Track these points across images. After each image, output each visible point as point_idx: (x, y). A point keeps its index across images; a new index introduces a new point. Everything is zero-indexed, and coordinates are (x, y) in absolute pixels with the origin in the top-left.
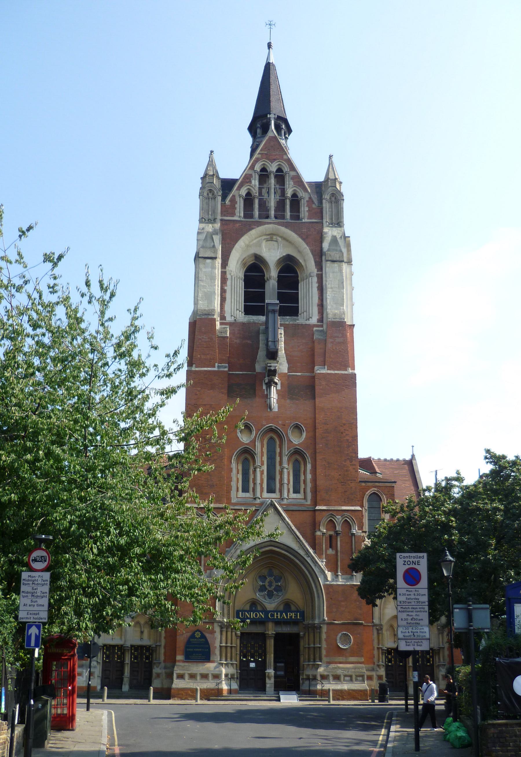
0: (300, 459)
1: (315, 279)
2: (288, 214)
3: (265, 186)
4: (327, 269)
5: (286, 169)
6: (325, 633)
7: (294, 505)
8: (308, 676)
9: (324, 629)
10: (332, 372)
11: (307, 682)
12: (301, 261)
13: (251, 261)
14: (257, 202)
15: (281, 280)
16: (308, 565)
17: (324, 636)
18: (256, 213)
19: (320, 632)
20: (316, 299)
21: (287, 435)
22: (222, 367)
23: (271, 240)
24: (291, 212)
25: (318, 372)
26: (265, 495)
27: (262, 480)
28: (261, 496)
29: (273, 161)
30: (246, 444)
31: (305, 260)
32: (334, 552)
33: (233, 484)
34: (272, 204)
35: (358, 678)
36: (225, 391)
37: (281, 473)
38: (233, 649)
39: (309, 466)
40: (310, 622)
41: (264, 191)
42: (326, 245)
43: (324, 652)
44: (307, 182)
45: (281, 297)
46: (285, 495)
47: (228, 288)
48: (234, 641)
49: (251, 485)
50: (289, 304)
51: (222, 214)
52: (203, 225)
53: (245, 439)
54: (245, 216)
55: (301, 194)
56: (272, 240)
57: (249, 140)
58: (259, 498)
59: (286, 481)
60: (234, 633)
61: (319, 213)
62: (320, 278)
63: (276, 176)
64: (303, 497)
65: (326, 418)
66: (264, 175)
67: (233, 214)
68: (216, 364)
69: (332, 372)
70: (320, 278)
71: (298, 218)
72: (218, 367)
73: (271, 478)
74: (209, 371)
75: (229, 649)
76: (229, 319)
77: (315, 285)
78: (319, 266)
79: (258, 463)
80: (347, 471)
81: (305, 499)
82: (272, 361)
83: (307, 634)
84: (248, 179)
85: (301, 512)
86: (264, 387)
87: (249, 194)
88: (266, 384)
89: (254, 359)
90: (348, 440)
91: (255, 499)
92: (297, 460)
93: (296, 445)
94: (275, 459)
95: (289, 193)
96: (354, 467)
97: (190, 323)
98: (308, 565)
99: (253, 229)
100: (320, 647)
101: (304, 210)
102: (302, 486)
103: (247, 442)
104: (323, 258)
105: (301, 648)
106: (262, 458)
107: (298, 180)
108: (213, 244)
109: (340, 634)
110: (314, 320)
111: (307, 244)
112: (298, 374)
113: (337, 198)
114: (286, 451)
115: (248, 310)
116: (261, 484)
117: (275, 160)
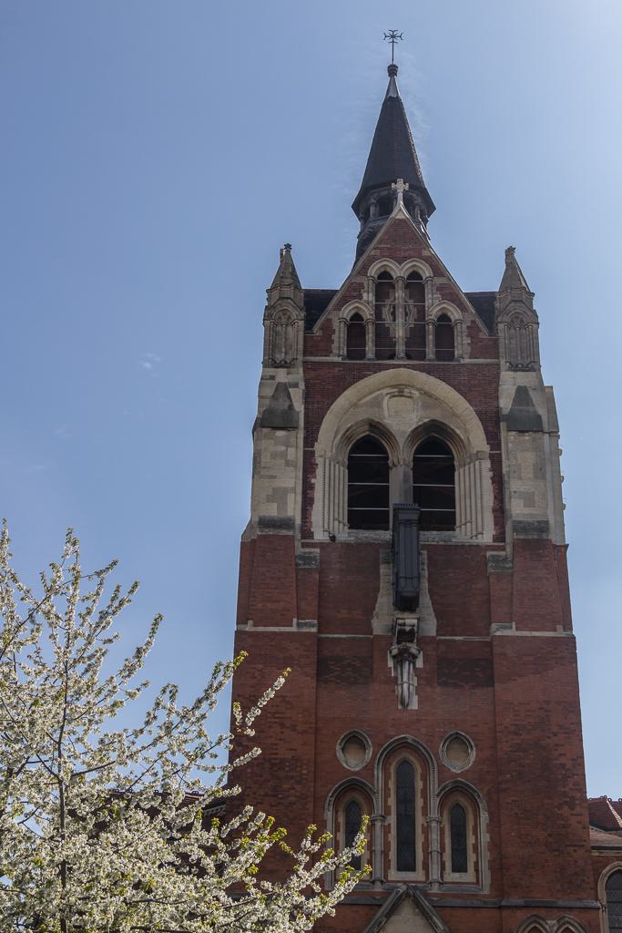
0: (463, 801)
1: (487, 464)
2: (430, 350)
3: (388, 302)
4: (510, 445)
5: (426, 272)
7: (455, 896)
12: (458, 432)
13: (363, 432)
14: (370, 330)
18: (370, 348)
20: (489, 500)
21: (436, 754)
22: (306, 624)
23: (401, 394)
24: (437, 345)
25: (498, 633)
26: (394, 875)
28: (386, 876)
29: (400, 261)
31: (466, 431)
34: (400, 332)
36: (312, 670)
37: (426, 830)
41: (386, 312)
42: (506, 403)
44: (466, 294)
45: (420, 496)
46: (435, 874)
47: (318, 481)
50: (435, 499)
51: (305, 354)
52: (271, 371)
53: (353, 762)
54: (350, 355)
55: (455, 314)
56: (401, 396)
57: (354, 226)
58: (382, 882)
59: (435, 846)
61: (492, 349)
62: (496, 462)
63: (407, 286)
64: (474, 880)
65: (518, 722)
66: (384, 284)
67: (328, 352)
68: (295, 620)
70: (496, 462)
71: (451, 356)
74: (281, 634)
76: (320, 536)
77: (488, 475)
78: (493, 439)
79: (379, 810)
80: (564, 827)
81: (478, 883)
82: (406, 615)
84: (355, 290)
85: (470, 909)
86: (391, 664)
87: (357, 317)
88: (394, 657)
89: (369, 611)
90: (563, 766)
91: (373, 882)
92: (458, 805)
93: (457, 775)
94: (412, 801)
95: (433, 312)
96: (579, 818)
97: (243, 544)
99: (366, 376)
101: (462, 345)
102: (471, 857)
104: (503, 425)
106: (386, 801)
107: (449, 291)
108: (287, 404)
110: (487, 538)
112: (457, 638)
113: (526, 322)
114: (434, 787)
115: (355, 521)
116: (385, 853)
117: (405, 258)
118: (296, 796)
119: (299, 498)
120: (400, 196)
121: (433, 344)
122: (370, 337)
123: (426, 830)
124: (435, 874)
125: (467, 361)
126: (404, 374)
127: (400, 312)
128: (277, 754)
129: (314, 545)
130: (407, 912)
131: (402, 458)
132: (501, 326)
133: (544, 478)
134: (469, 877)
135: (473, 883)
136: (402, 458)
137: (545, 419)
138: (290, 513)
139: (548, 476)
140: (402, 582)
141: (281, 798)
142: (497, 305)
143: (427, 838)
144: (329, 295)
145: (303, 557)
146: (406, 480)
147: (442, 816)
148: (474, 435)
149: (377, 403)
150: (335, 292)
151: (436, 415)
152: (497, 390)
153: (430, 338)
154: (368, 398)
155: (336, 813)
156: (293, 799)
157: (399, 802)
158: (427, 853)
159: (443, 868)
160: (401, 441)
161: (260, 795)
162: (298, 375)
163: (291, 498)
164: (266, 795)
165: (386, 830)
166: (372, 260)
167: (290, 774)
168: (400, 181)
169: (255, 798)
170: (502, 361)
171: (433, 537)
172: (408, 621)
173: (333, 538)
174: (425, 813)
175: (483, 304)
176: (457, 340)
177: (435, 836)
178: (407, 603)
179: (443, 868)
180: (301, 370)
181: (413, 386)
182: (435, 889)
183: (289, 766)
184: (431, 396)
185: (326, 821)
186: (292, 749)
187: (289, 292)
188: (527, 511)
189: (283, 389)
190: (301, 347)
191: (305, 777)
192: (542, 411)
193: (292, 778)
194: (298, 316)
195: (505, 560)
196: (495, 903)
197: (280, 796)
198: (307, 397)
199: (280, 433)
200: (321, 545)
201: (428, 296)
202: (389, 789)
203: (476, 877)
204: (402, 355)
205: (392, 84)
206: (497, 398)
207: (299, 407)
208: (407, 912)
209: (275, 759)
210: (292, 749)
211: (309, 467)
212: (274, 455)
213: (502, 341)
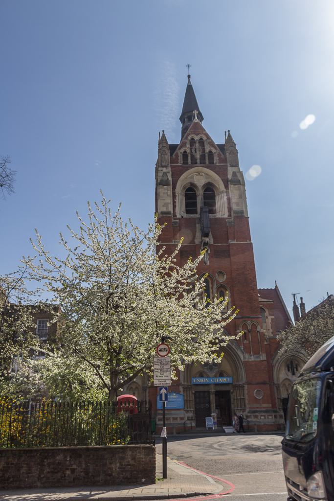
3: (194, 147)
5: (205, 138)
9: (246, 387)
10: (239, 242)
12: (216, 185)
13: (189, 186)
14: (189, 155)
15: (206, 197)
17: (246, 392)
18: (189, 161)
19: (243, 390)
21: (215, 277)
24: (209, 160)
25: (231, 243)
31: (218, 185)
32: (248, 342)
34: (198, 156)
35: (269, 417)
38: (191, 401)
40: (237, 383)
41: (193, 150)
42: (230, 177)
43: (247, 402)
47: (177, 200)
51: (171, 163)
55: (214, 151)
61: (224, 160)
63: (199, 143)
67: (178, 163)
69: (239, 242)
71: (213, 163)
72: (174, 242)
75: (188, 402)
76: (178, 216)
78: (226, 187)
82: (205, 238)
87: (185, 152)
90: (251, 279)
92: (222, 291)
95: (207, 150)
98: (233, 350)
100: (244, 399)
101: (216, 159)
104: (229, 183)
105: (232, 400)
107: (212, 144)
109: (256, 391)
110: (226, 216)
111: (219, 176)
113: (235, 153)
114: (215, 286)
115: (188, 212)
119: (172, 206)
120: (196, 115)
121: (207, 160)
122: (189, 158)
125: (218, 164)
126: (200, 169)
127: (197, 150)
129: (177, 219)
131: (200, 193)
132: (227, 154)
133: (242, 198)
136: (200, 193)
137: (241, 181)
138: (170, 210)
139: (243, 198)
140: (205, 229)
142: (225, 148)
144: (177, 146)
145: (173, 223)
146: (202, 200)
148: (221, 186)
149: (192, 177)
150: (178, 145)
151: (210, 180)
152: (227, 173)
153: (207, 158)
154: (190, 176)
160: (200, 188)
162: (169, 169)
163: (170, 205)
166: (189, 135)
168: (196, 111)
170: (228, 164)
171: (211, 216)
172: (206, 240)
173: (182, 217)
174: (213, 293)
175: (221, 147)
176: (215, 158)
178: (206, 235)
180: (170, 168)
181: (202, 172)
184: (208, 175)
187: (165, 145)
188: (238, 207)
189: (165, 174)
190: (169, 161)
192: (240, 178)
194: (168, 152)
195: (232, 222)
198: (172, 176)
199: (165, 187)
200: (179, 219)
201: (206, 145)
204: (199, 163)
205: (189, 80)
206: (227, 175)
207: (170, 179)
211: (174, 196)
212: (164, 193)
213: (228, 158)
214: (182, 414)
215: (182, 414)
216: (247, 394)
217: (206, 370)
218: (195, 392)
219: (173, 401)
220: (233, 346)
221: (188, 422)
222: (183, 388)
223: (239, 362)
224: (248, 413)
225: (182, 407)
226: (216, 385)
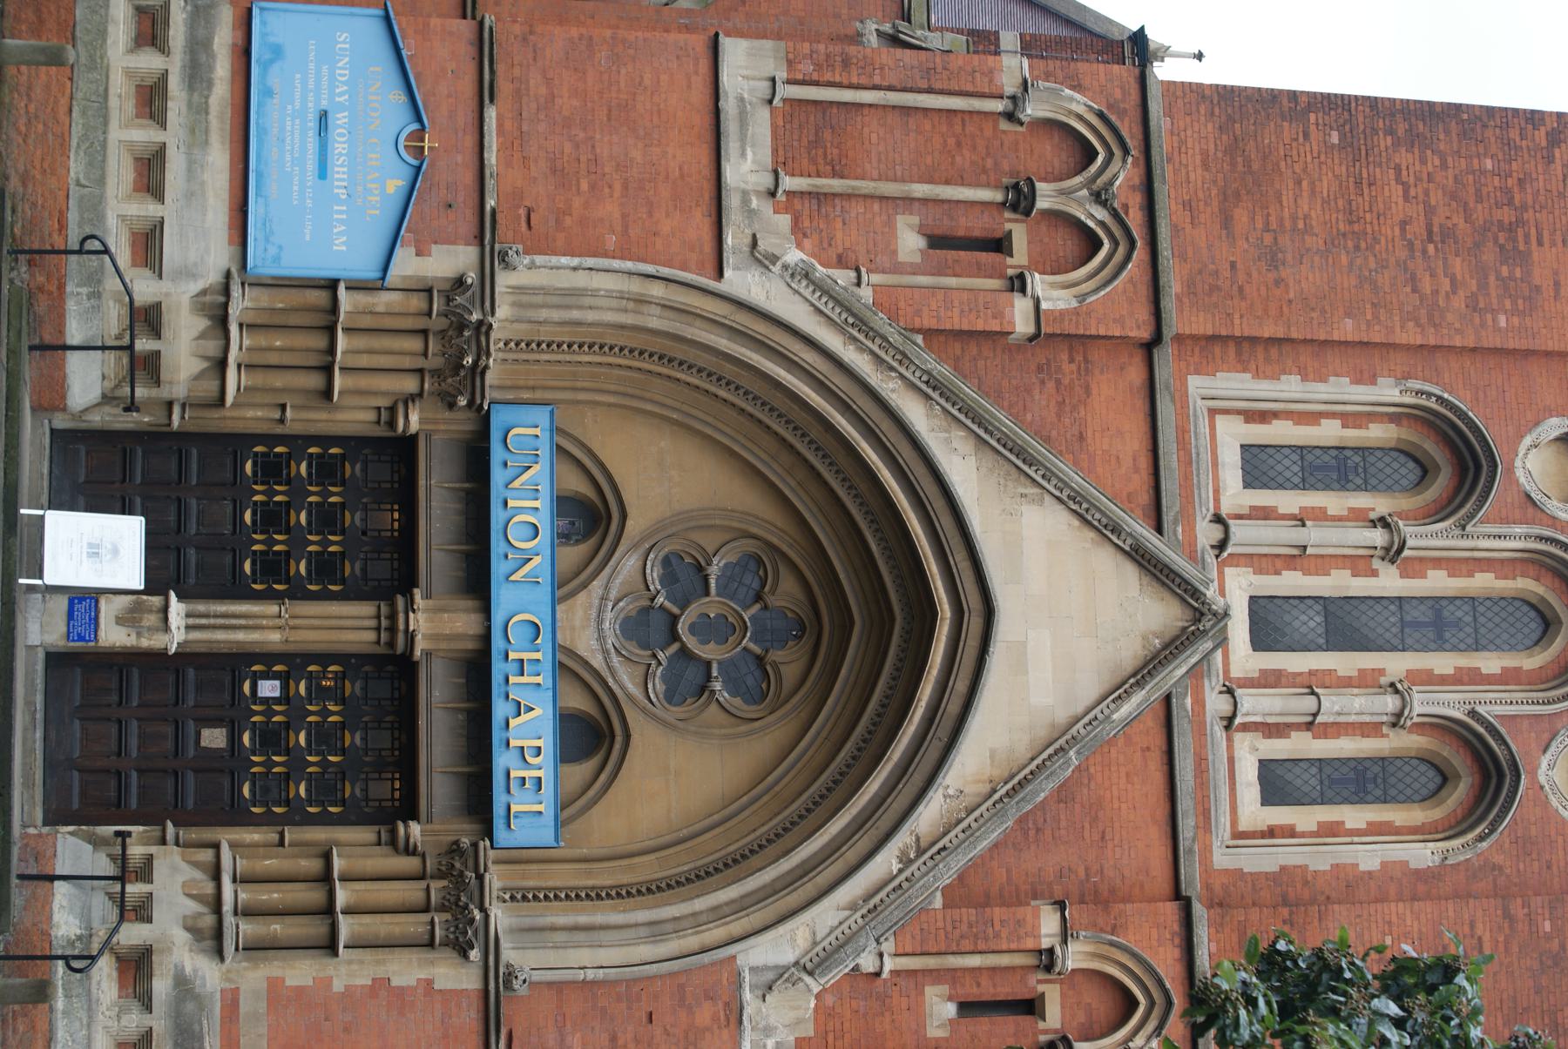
6: (429, 983)
8: (145, 872)
9: (456, 976)
11: (102, 864)
16: (851, 855)
17: (405, 970)
19: (431, 944)
27: (1322, 564)
28: (1236, 560)
30: (1510, 470)
33: (1290, 387)
37: (1367, 681)
39: (1423, 855)
43: (301, 972)
46: (1253, 704)
48: (364, 382)
49: (1289, 501)
58: (1221, 546)
60: (410, 384)
64: (1243, 826)
73: (1343, 624)
79: (1420, 538)
81: (1238, 835)
83: (410, 864)
85: (1162, 812)
92: (1445, 778)
93: (1533, 773)
94: (1440, 644)
98: (851, 855)
102: (1305, 817)
103: (1520, 474)
106: (1437, 563)
114: (1496, 705)
116: (1298, 558)
118: (1436, 292)
123: (1367, 681)
124: (1253, 704)
128: (1540, 244)
130: (1157, 614)
134: (1253, 811)
135: (1234, 822)
141: (1424, 252)
143: (1346, 683)
147: (1419, 728)
155: (1394, 418)
156: (1426, 286)
157: (1436, 603)
158: (1310, 684)
159: (1273, 730)
161: (1427, 193)
164: (1430, 211)
165: (1359, 563)
167: (1492, 278)
169: (1418, 179)
177: (1360, 705)
179: (1273, 730)
182: (1216, 704)
183: (1511, 278)
185: (1373, 382)
186: (1557, 284)
191: (1490, 322)
193: (1483, 286)
196: (1190, 883)
197: (1431, 248)
202: (1470, 574)
203: (1244, 829)
208: (1157, 614)
209: (1527, 236)
210: (1557, 284)
214: (199, 247)
215: (199, 247)
216: (381, 984)
217: (627, 565)
218: (408, 444)
219: (323, 172)
220: (886, 862)
221: (113, 320)
222: (459, 283)
223: (718, 914)
224: (183, 984)
225: (261, 260)
226: (476, 671)
